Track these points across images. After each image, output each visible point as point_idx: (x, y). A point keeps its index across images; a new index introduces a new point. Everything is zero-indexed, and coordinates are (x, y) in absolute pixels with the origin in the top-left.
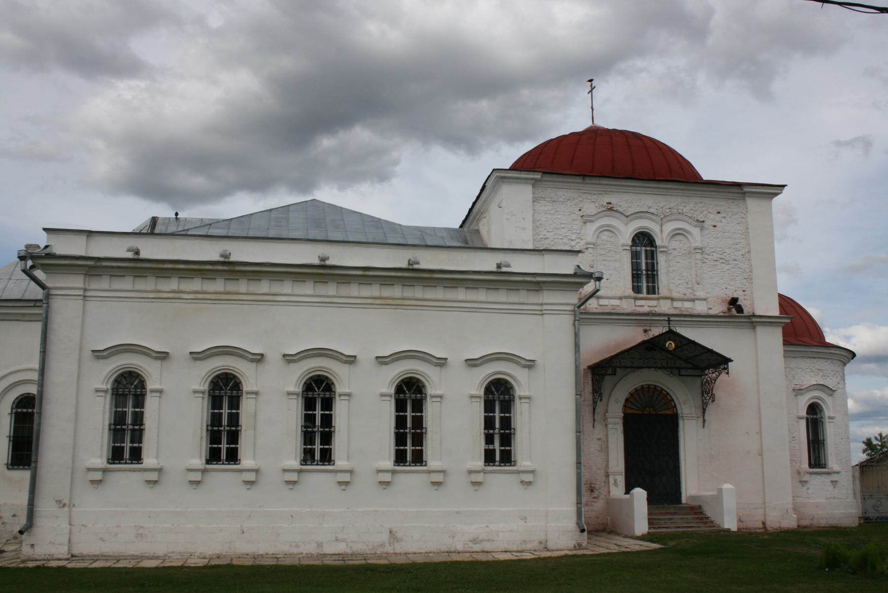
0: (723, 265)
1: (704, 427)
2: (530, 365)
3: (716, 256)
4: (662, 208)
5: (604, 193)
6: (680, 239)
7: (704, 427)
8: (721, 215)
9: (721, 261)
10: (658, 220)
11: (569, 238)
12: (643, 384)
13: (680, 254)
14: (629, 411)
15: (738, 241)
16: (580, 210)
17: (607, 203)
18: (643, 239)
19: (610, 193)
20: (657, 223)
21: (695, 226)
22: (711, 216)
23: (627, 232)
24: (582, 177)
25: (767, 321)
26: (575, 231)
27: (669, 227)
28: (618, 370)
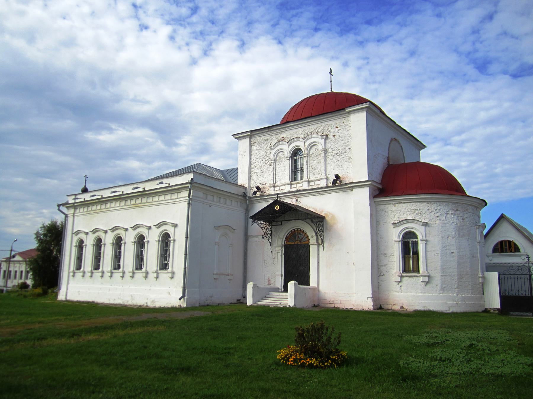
0: (339, 157)
1: (323, 250)
2: (176, 226)
3: (335, 152)
4: (307, 133)
5: (281, 133)
6: (316, 148)
7: (323, 250)
8: (338, 129)
9: (337, 154)
10: (302, 140)
11: (265, 159)
12: (301, 228)
13: (315, 156)
14: (288, 243)
15: (346, 141)
16: (270, 144)
17: (282, 138)
18: (296, 152)
19: (284, 132)
20: (302, 142)
21: (321, 139)
22: (333, 130)
23: (287, 150)
24: (267, 128)
25: (359, 185)
26: (267, 156)
27: (307, 143)
28: (283, 222)
